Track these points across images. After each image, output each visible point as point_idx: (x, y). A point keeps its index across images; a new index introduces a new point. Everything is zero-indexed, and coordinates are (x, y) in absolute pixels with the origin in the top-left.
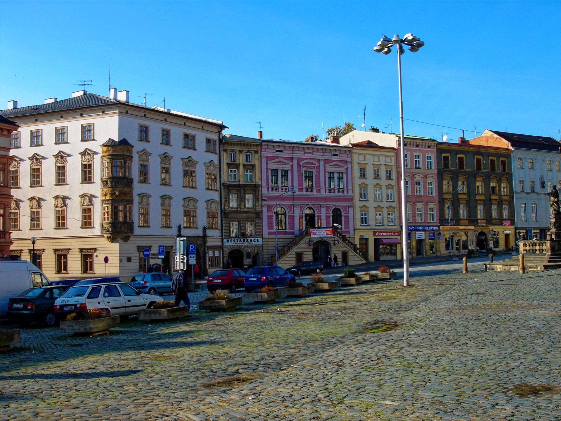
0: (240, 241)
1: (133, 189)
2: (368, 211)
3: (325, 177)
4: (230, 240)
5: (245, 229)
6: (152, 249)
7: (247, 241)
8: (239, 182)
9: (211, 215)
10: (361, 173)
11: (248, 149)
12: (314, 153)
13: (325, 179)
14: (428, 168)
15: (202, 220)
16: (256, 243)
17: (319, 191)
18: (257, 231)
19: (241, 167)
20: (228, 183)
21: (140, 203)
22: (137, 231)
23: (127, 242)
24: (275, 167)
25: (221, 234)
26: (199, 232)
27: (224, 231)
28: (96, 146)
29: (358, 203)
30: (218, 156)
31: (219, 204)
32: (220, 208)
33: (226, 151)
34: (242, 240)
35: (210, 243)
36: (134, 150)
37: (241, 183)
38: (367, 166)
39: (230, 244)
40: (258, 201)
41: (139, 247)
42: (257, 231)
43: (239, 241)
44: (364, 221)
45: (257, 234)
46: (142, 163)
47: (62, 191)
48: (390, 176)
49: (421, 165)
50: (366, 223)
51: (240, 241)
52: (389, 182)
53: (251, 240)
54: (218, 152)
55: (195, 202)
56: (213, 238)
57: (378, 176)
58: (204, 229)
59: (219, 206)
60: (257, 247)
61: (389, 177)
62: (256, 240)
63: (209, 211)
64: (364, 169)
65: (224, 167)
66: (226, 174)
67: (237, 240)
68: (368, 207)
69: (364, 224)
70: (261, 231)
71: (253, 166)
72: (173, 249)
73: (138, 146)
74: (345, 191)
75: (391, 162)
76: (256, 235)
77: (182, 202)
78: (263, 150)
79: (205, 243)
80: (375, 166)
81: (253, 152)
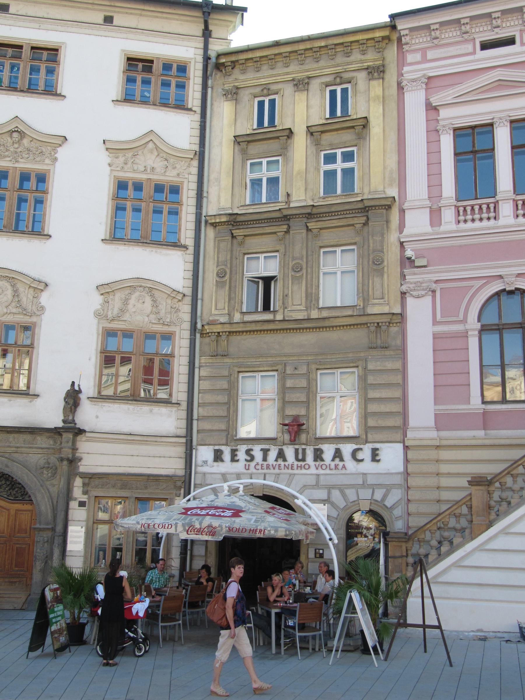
0: (281, 455)
7: (318, 455)
8: (288, 202)
16: (368, 466)
25: (183, 424)
30: (197, 117)
31: (188, 300)
32: (187, 317)
34: (289, 452)
37: (292, 205)
40: (380, 272)
42: (373, 408)
45: (371, 422)
51: (281, 455)
53: (338, 454)
59: (186, 308)
60: (374, 487)
62: (366, 454)
66: (226, 182)
67: (265, 452)
70: (396, 408)
76: (366, 428)
78: (410, 58)
81: (362, 76)
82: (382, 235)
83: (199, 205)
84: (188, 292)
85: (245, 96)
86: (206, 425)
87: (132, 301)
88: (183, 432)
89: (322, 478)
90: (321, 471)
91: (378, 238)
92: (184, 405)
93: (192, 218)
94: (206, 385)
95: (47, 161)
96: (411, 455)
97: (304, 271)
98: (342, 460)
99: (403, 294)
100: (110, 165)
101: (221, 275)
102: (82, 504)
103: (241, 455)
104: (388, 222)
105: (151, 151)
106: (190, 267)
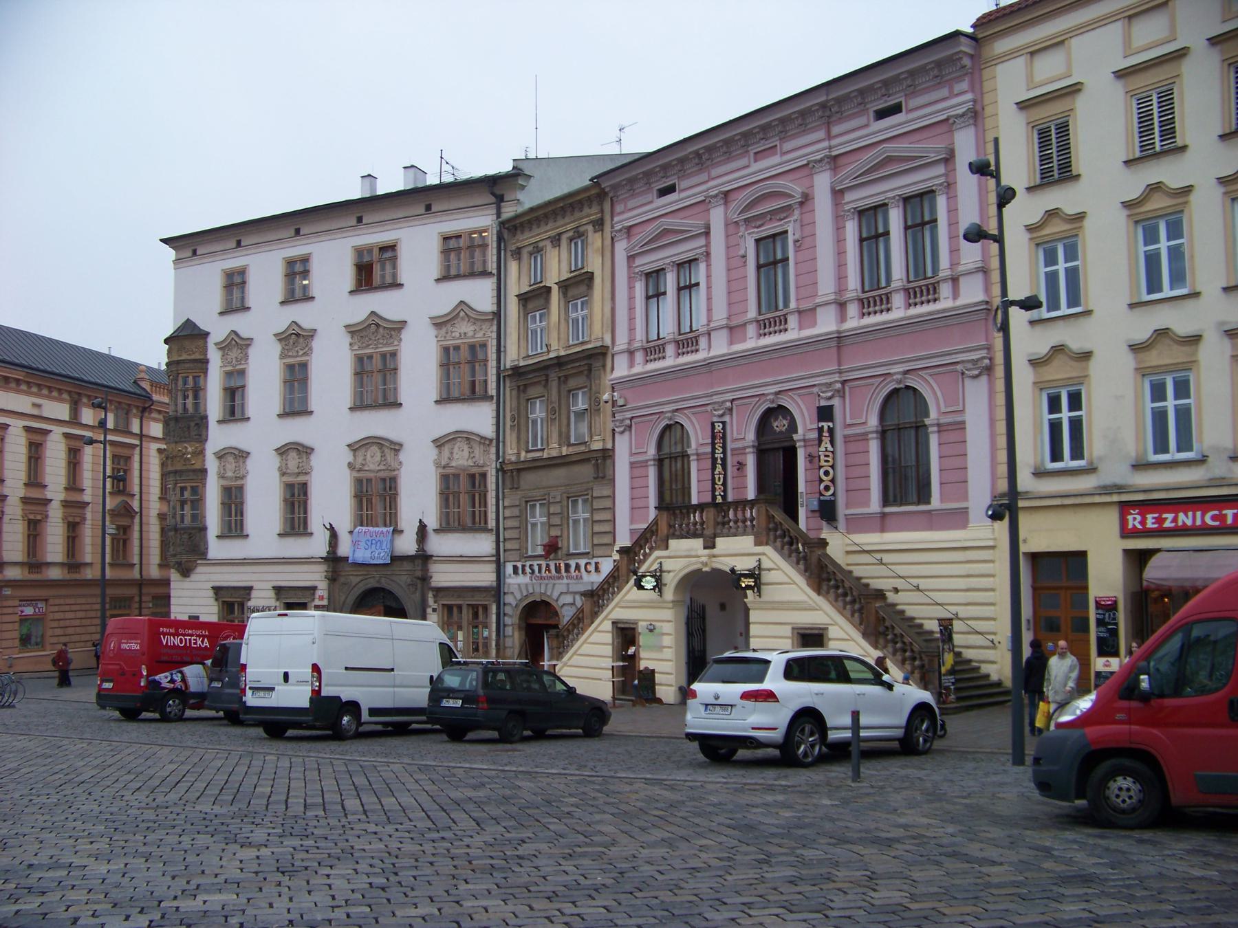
3: (840, 241)
6: (254, 594)
7: (567, 567)
10: (1045, 159)
11: (570, 226)
12: (788, 146)
13: (840, 253)
17: (807, 315)
18: (597, 528)
21: (222, 476)
22: (217, 548)
23: (189, 577)
24: (648, 262)
25: (494, 545)
26: (407, 544)
30: (494, 279)
33: (517, 254)
35: (442, 576)
36: (211, 341)
38: (1081, 103)
39: (522, 579)
41: (217, 590)
42: (597, 528)
45: (596, 542)
46: (229, 368)
50: (1077, 453)
53: (578, 567)
54: (492, 266)
55: (390, 456)
58: (422, 530)
64: (1063, 129)
69: (1067, 463)
72: (317, 596)
73: (218, 329)
74: (945, 290)
76: (594, 545)
77: (348, 457)
79: (425, 579)
80: (1140, 82)
81: (590, 228)
82: (600, 378)
85: (525, 253)
86: (509, 545)
88: (494, 552)
89: (570, 586)
90: (569, 581)
91: (597, 382)
93: (494, 371)
94: (508, 513)
95: (396, 343)
97: (557, 414)
98: (579, 571)
100: (436, 337)
101: (513, 419)
102: (434, 610)
103: (528, 570)
104: (604, 366)
105: (463, 319)
106: (494, 414)
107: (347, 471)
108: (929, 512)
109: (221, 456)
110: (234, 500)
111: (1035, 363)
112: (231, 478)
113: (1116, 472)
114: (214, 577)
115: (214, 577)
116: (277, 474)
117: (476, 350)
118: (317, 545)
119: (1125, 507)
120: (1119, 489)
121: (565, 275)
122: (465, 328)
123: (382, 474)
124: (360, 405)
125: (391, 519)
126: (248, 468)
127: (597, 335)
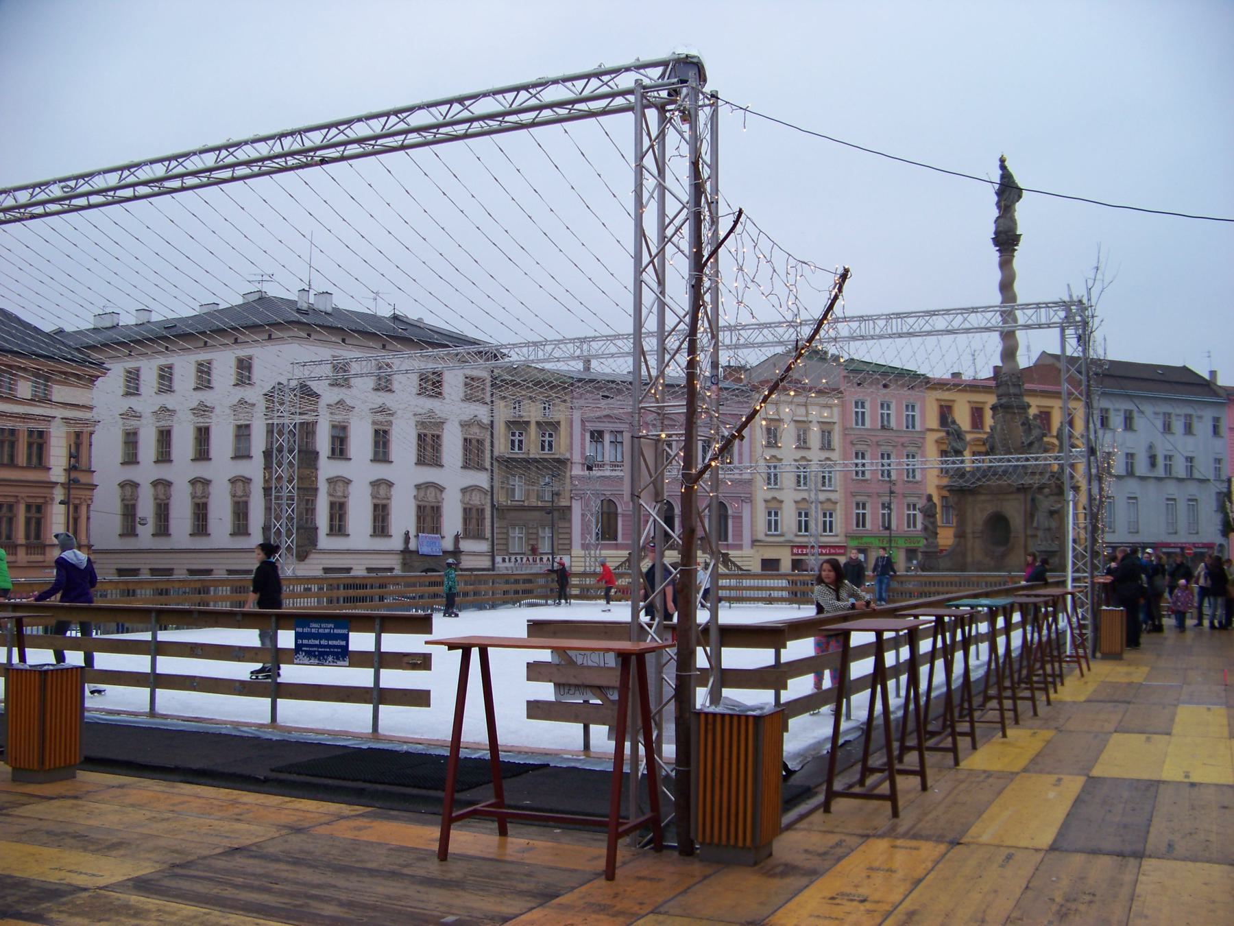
0: (528, 559)
1: (317, 469)
2: (780, 508)
4: (507, 558)
5: (537, 539)
7: (541, 559)
8: (528, 454)
9: (472, 517)
14: (907, 427)
15: (452, 521)
19: (533, 426)
20: (507, 456)
21: (330, 495)
22: (324, 541)
23: (303, 560)
25: (490, 547)
26: (448, 544)
27: (495, 542)
28: (254, 394)
29: (762, 491)
31: (489, 493)
32: (489, 501)
34: (531, 558)
35: (467, 562)
36: (323, 402)
39: (507, 564)
43: (525, 560)
44: (773, 525)
47: (201, 470)
48: (829, 443)
49: (893, 424)
51: (528, 559)
52: (826, 454)
54: (488, 400)
55: (438, 493)
56: (474, 554)
57: (805, 442)
58: (457, 538)
61: (827, 446)
63: (469, 506)
65: (500, 429)
66: (502, 440)
67: (522, 559)
68: (781, 502)
71: (555, 425)
73: (329, 395)
75: (832, 417)
77: (414, 492)
83: (492, 451)
84: (489, 490)
86: (499, 547)
87: (473, 495)
88: (490, 550)
92: (490, 539)
94: (499, 531)
96: (573, 559)
99: (571, 498)
107: (413, 501)
108: (727, 545)
109: (331, 481)
110: (338, 512)
111: (766, 501)
112: (338, 497)
113: (789, 536)
114: (323, 561)
115: (323, 561)
116: (370, 497)
117: (480, 442)
118: (396, 543)
119: (792, 547)
120: (791, 541)
121: (540, 419)
122: (475, 430)
123: (433, 504)
124: (421, 461)
125: (436, 529)
126: (350, 491)
127: (561, 451)
